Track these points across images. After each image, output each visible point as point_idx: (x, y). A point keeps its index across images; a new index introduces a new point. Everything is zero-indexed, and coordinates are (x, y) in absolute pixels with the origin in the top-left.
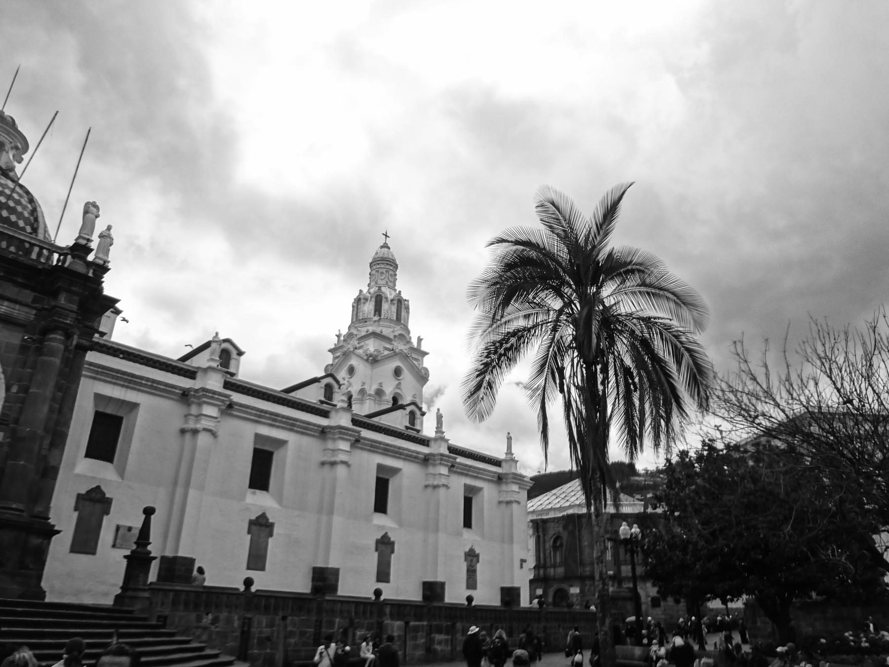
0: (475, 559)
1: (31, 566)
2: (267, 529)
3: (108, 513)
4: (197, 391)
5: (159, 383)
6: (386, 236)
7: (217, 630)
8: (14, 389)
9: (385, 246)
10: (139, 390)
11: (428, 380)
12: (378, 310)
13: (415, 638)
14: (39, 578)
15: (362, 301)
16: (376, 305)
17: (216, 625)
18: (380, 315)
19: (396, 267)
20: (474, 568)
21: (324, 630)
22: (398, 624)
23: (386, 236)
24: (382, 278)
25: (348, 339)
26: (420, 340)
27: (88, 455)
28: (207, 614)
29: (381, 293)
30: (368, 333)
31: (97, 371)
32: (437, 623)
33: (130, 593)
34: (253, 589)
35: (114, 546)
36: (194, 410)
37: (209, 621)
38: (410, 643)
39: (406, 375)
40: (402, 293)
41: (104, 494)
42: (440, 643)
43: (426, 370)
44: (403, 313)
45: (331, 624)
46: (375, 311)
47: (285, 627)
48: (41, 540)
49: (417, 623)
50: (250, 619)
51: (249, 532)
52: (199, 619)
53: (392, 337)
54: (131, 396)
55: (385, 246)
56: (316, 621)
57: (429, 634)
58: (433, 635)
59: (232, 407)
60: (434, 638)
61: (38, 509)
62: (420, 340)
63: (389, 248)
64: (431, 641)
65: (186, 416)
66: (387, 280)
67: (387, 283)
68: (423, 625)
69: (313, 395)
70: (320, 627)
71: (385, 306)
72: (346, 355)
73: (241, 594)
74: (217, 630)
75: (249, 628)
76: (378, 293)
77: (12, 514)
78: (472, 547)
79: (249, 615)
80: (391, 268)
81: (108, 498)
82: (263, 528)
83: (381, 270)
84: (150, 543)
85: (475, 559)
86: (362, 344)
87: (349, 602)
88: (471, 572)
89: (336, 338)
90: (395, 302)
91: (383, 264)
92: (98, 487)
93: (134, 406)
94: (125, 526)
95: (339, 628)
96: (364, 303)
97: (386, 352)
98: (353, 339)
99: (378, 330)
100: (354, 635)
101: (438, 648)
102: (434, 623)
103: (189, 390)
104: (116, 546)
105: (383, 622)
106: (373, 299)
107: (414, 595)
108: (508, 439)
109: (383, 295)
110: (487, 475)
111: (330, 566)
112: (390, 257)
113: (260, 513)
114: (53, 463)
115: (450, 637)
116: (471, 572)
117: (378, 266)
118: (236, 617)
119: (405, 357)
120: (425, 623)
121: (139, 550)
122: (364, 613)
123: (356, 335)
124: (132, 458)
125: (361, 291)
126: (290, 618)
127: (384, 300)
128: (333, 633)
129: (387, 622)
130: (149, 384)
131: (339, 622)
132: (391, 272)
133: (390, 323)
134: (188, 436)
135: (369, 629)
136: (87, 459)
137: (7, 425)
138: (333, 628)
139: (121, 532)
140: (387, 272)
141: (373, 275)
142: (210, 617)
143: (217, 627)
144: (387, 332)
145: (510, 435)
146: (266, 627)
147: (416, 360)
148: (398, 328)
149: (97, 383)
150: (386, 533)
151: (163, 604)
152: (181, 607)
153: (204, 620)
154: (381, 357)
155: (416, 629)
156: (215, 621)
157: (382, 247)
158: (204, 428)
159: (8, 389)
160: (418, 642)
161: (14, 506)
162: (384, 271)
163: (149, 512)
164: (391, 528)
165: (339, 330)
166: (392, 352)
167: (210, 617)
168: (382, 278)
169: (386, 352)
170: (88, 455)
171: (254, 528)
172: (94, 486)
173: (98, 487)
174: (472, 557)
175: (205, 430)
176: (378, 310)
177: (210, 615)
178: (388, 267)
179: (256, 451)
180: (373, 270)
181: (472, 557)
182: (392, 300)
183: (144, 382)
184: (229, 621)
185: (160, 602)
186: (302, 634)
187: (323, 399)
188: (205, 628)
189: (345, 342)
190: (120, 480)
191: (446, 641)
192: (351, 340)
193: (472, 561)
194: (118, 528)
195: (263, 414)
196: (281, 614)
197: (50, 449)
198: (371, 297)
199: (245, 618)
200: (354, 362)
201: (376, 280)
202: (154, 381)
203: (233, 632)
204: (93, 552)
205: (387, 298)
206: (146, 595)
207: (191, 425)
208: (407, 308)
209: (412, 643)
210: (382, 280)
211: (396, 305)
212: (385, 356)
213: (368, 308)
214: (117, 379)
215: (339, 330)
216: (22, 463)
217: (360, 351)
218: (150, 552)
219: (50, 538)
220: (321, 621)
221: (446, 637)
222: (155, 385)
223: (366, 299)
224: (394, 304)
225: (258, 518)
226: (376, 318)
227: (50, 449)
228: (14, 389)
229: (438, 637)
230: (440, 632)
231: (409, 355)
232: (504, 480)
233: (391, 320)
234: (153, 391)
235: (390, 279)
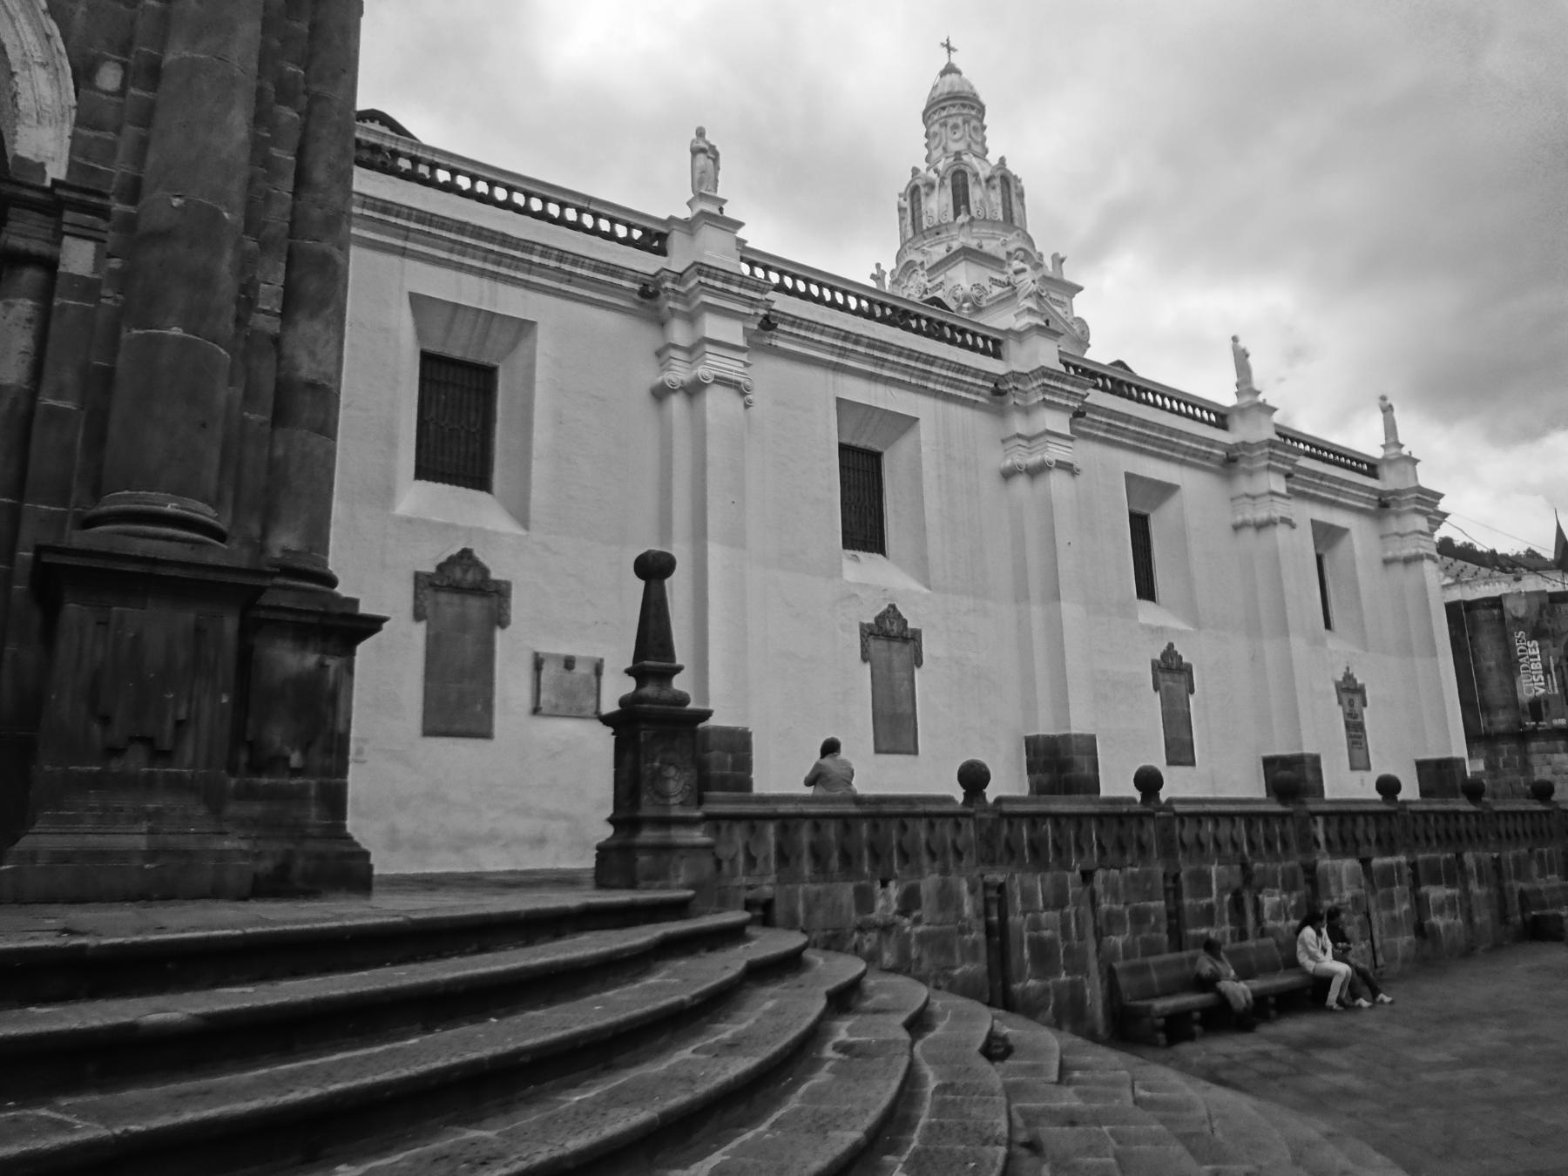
0: (1357, 699)
1: (295, 759)
2: (908, 648)
3: (504, 624)
4: (679, 277)
5: (577, 260)
6: (949, 49)
7: (920, 929)
8: (109, 78)
9: (950, 69)
10: (527, 285)
11: (1089, 346)
13: (1389, 903)
14: (335, 801)
15: (923, 190)
17: (915, 914)
19: (981, 110)
20: (1359, 720)
21: (1187, 901)
22: (1348, 865)
23: (949, 49)
24: (958, 136)
25: (902, 279)
27: (423, 472)
28: (884, 884)
29: (962, 167)
30: (951, 252)
31: (408, 229)
32: (1428, 855)
33: (648, 836)
34: (991, 793)
35: (536, 711)
36: (679, 333)
37: (895, 906)
38: (1379, 917)
40: (1007, 162)
41: (485, 571)
42: (1440, 910)
43: (1081, 321)
44: (1016, 208)
45: (1201, 881)
47: (1094, 903)
48: (311, 660)
49: (1388, 860)
50: (1001, 888)
51: (865, 659)
52: (864, 900)
53: (1003, 256)
54: (511, 302)
55: (950, 69)
56: (1165, 876)
57: (1416, 883)
58: (1424, 889)
59: (774, 327)
60: (1427, 896)
61: (285, 541)
63: (958, 72)
64: (1420, 903)
65: (659, 354)
66: (968, 139)
67: (969, 146)
68: (1399, 866)
70: (1178, 893)
71: (975, 193)
73: (956, 818)
74: (920, 929)
75: (1003, 917)
76: (955, 167)
77: (170, 539)
78: (1348, 669)
79: (998, 877)
80: (973, 113)
81: (497, 582)
82: (896, 645)
83: (951, 122)
84: (679, 669)
85: (1357, 699)
87: (1231, 816)
88: (1355, 729)
90: (997, 182)
91: (953, 106)
92: (466, 554)
93: (525, 328)
94: (556, 657)
95: (1222, 891)
96: (927, 195)
97: (997, 290)
98: (914, 275)
99: (973, 244)
100: (1258, 907)
101: (1438, 921)
102: (1420, 857)
103: (657, 278)
104: (543, 711)
105: (1315, 864)
106: (948, 182)
107: (1248, 786)
108: (1384, 411)
109: (968, 170)
110: (1356, 498)
111: (1074, 731)
112: (967, 89)
113: (885, 607)
114: (306, 369)
115: (1456, 892)
116: (1355, 729)
117: (944, 113)
118: (964, 886)
120: (1402, 859)
121: (650, 690)
122: (1270, 845)
123: (922, 263)
124: (540, 470)
125: (915, 171)
126: (1100, 874)
127: (971, 180)
128: (1210, 907)
129: (1325, 862)
130: (553, 264)
131: (1219, 876)
132: (974, 123)
133: (992, 228)
134: (676, 403)
135: (1289, 887)
136: (423, 483)
137: (103, 212)
138: (1210, 895)
139: (548, 672)
140: (965, 122)
141: (935, 134)
142: (894, 890)
143: (917, 921)
144: (990, 247)
145: (1388, 402)
146: (1046, 907)
147: (1061, 304)
148: (1010, 237)
149: (411, 264)
150: (1171, 646)
151: (751, 861)
152: (807, 868)
153: (880, 903)
154: (988, 301)
155: (1387, 876)
156: (910, 901)
157: (943, 73)
158: (716, 377)
159: (84, 75)
160: (1396, 912)
161: (170, 508)
162: (959, 121)
163: (654, 569)
164: (1180, 633)
165: (878, 266)
166: (1007, 288)
167: (894, 890)
168: (958, 136)
169: (997, 290)
170: (423, 472)
171: (877, 646)
172: (455, 550)
173: (466, 554)
174: (1350, 691)
175: (720, 381)
176: (961, 199)
177: (892, 884)
178: (965, 111)
179: (844, 449)
180: (933, 124)
181: (1350, 691)
182: (988, 180)
183: (536, 259)
184: (947, 898)
185: (741, 858)
186: (1140, 918)
188: (886, 929)
189: (896, 286)
190: (521, 532)
191: (1451, 902)
192: (909, 280)
193: (1351, 703)
194: (538, 663)
195: (849, 346)
196: (1077, 866)
197: (287, 314)
198: (942, 179)
199: (986, 886)
201: (943, 143)
202: (562, 256)
203: (962, 931)
204: (484, 732)
205: (976, 175)
206: (698, 836)
207: (679, 373)
208: (1021, 195)
209: (1385, 914)
210: (956, 141)
211: (998, 190)
212: (994, 298)
213: (938, 204)
214: (463, 254)
215: (878, 266)
216: (176, 331)
218: (683, 699)
219: (348, 651)
220: (1176, 878)
221: (1449, 892)
222: (567, 267)
223: (931, 186)
224: (994, 188)
225: (880, 619)
227: (287, 314)
228: (109, 78)
229: (1436, 893)
230: (1435, 880)
231: (1044, 294)
232: (1393, 508)
233: (994, 222)
234: (564, 287)
235: (974, 136)
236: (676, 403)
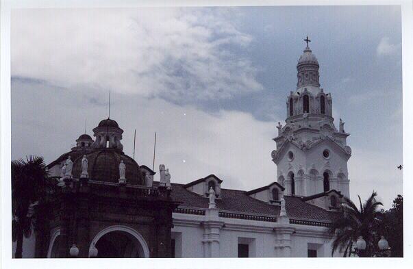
9: (308, 51)
12: (306, 107)
15: (294, 101)
16: (304, 102)
18: (308, 112)
26: (342, 124)
39: (332, 153)
44: (327, 105)
46: (304, 109)
53: (319, 129)
55: (308, 51)
62: (342, 124)
69: (265, 197)
72: (287, 144)
86: (297, 136)
89: (277, 129)
90: (319, 99)
99: (306, 126)
106: (302, 99)
117: (303, 69)
119: (330, 142)
125: (292, 92)
134: (206, 245)
144: (315, 124)
147: (341, 142)
148: (323, 120)
157: (305, 51)
159: (150, 250)
165: (279, 123)
176: (306, 107)
187: (272, 200)
200: (292, 149)
207: (206, 239)
208: (330, 101)
213: (299, 106)
215: (279, 123)
217: (296, 142)
226: (305, 115)
228: (152, 250)
236: (206, 245)
